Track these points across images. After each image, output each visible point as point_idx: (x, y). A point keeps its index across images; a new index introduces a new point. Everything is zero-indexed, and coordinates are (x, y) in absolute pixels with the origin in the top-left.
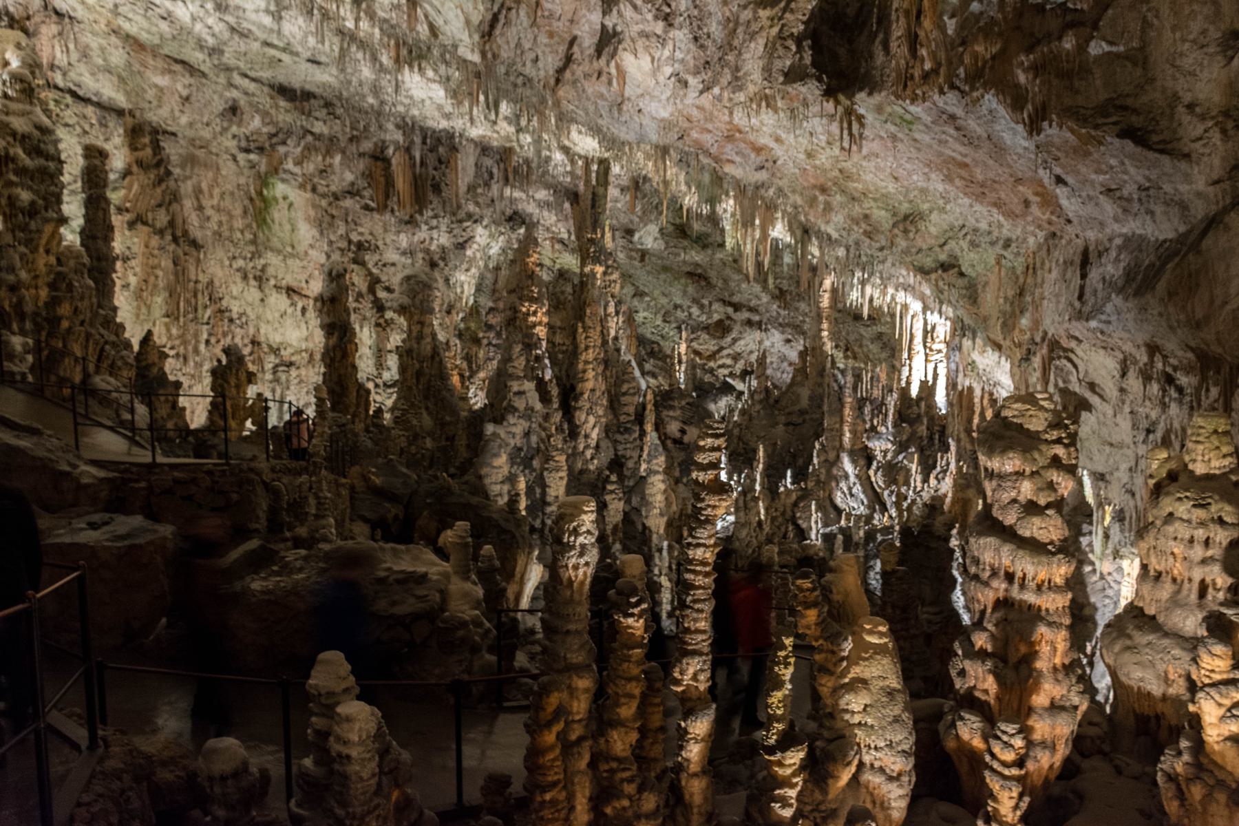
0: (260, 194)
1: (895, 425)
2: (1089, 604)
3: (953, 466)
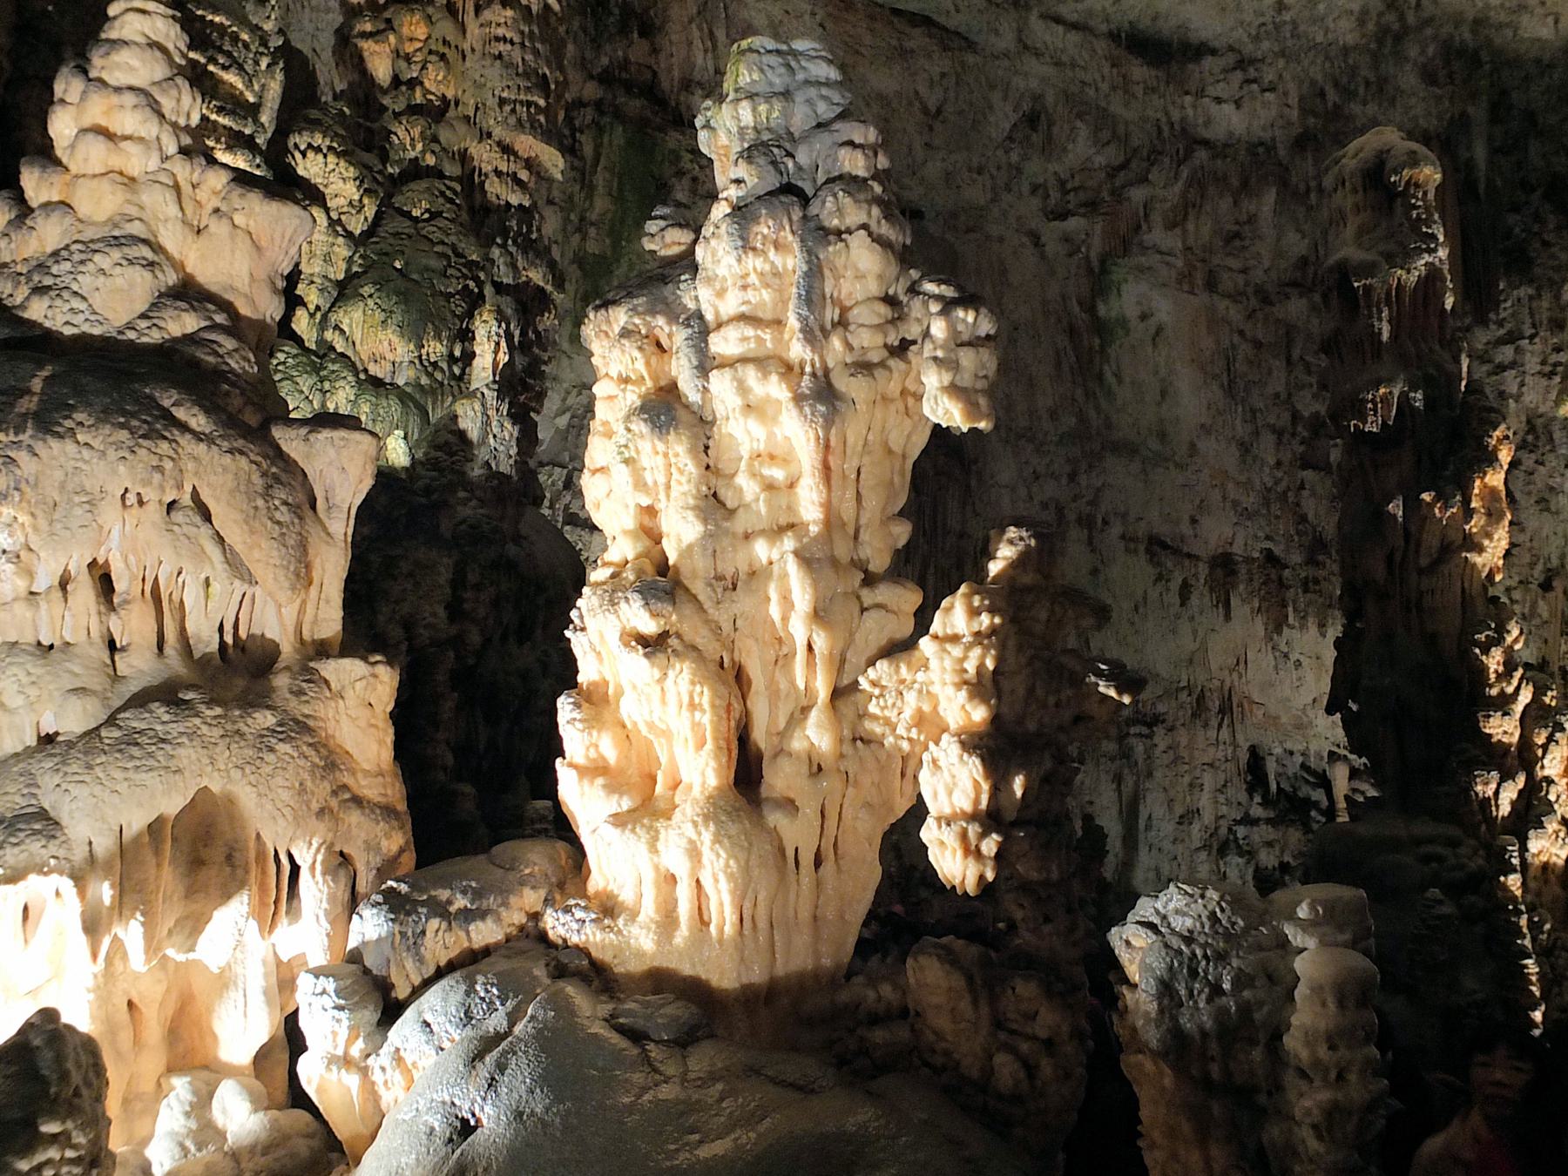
0: (1091, 310)
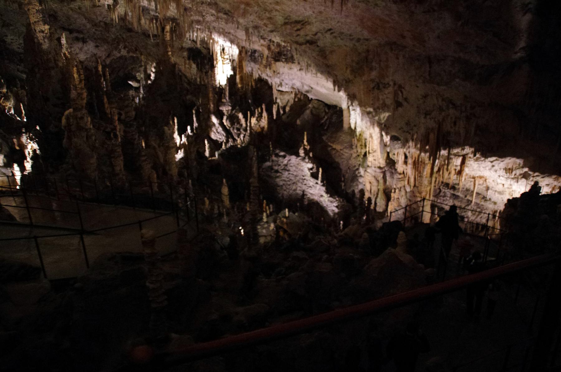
1: (230, 98)
2: (335, 162)
3: (265, 114)
